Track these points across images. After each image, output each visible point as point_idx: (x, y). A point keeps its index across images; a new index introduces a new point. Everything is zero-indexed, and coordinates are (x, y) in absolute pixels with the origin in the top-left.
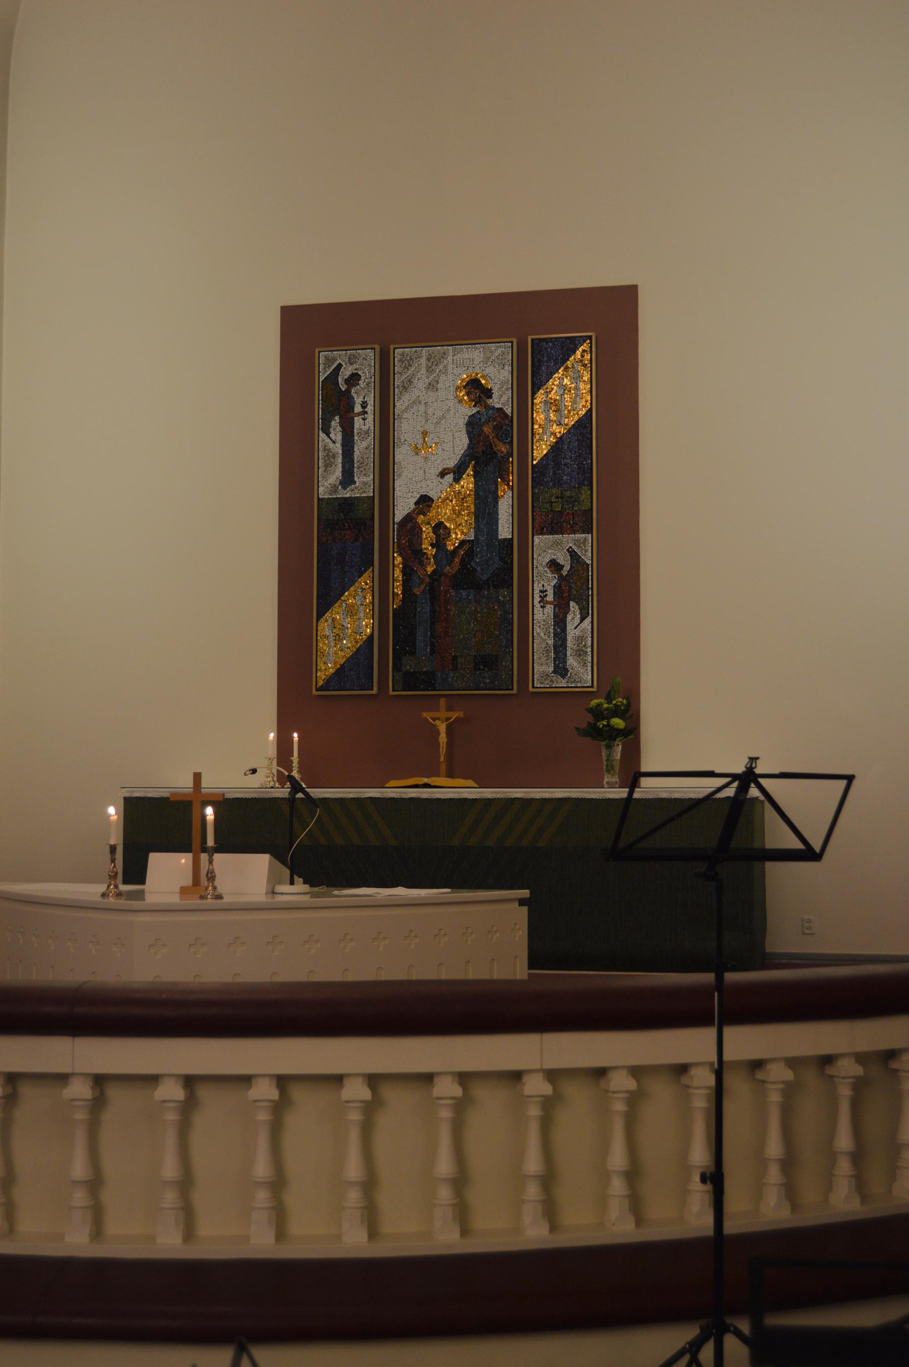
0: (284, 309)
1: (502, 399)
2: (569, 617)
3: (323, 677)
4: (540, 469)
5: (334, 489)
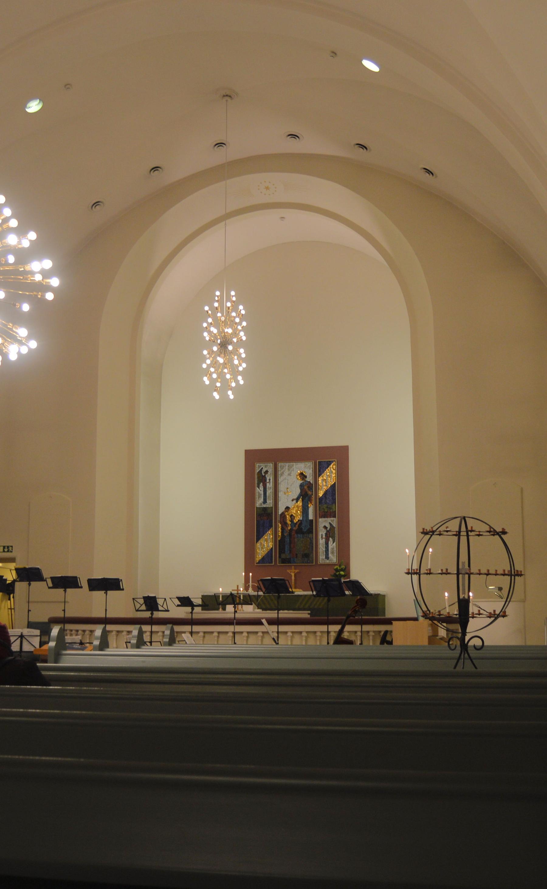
0: (246, 451)
1: (310, 479)
2: (329, 542)
3: (258, 560)
4: (321, 499)
5: (261, 504)
